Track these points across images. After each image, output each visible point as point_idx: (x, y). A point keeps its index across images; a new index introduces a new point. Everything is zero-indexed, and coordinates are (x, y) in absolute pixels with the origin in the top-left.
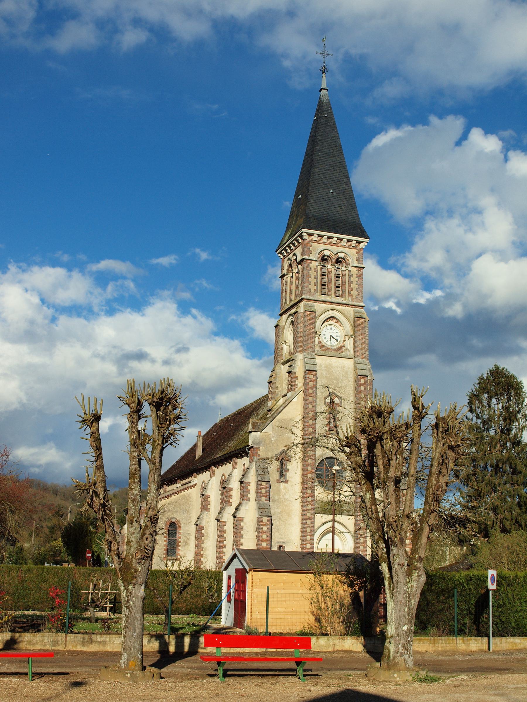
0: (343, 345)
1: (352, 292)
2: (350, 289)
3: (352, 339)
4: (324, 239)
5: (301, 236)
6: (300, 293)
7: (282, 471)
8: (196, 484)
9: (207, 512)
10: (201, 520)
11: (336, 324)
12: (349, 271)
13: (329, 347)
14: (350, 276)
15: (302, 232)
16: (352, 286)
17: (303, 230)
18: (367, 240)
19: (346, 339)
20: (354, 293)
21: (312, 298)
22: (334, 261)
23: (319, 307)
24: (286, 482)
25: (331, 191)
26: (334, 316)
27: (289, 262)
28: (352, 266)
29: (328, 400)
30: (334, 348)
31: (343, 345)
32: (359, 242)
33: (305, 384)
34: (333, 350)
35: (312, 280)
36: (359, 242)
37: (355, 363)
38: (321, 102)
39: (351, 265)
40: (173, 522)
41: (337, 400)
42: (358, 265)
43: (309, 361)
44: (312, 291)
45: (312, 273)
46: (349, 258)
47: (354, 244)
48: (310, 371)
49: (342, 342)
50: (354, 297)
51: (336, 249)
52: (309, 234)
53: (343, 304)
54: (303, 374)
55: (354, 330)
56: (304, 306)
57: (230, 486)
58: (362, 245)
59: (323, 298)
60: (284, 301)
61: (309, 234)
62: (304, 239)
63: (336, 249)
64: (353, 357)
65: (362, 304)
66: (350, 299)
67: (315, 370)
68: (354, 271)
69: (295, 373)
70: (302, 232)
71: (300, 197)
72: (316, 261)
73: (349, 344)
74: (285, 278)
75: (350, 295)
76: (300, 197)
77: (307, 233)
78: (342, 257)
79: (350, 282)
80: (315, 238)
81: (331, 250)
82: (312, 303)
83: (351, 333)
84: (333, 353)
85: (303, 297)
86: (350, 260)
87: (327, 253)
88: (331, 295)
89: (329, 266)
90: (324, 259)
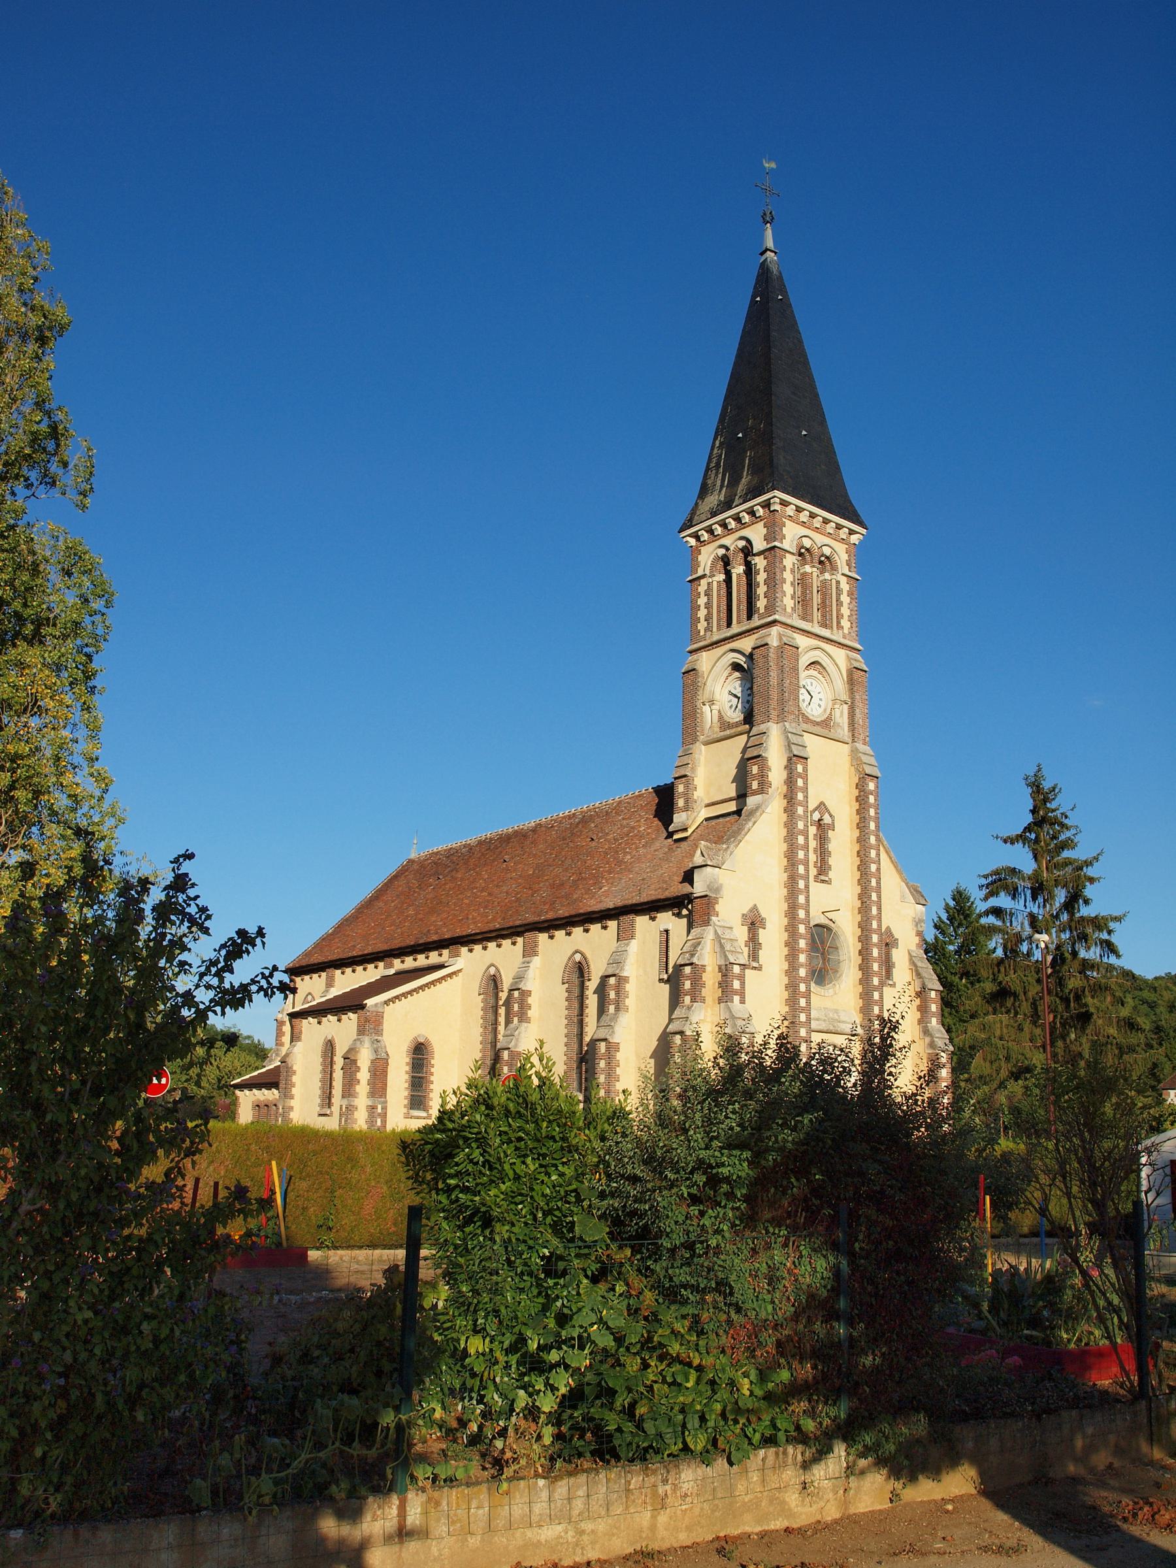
0: (829, 718)
3: (846, 707)
4: (804, 517)
5: (767, 505)
6: (762, 610)
7: (754, 942)
8: (460, 971)
9: (524, 1025)
10: (517, 1040)
11: (820, 676)
12: (838, 582)
13: (811, 717)
14: (839, 591)
15: (775, 497)
17: (777, 493)
18: (864, 531)
19: (836, 706)
20: (845, 623)
21: (789, 621)
22: (816, 560)
23: (802, 641)
24: (759, 968)
25: (804, 433)
26: (820, 661)
27: (722, 552)
28: (843, 574)
29: (816, 816)
30: (818, 720)
31: (829, 718)
32: (852, 532)
33: (790, 782)
34: (818, 724)
35: (788, 589)
36: (852, 532)
37: (854, 753)
38: (764, 269)
40: (422, 1044)
41: (827, 819)
42: (850, 574)
43: (793, 738)
44: (789, 610)
45: (788, 576)
46: (837, 558)
48: (795, 759)
49: (828, 712)
50: (846, 631)
51: (820, 539)
52: (784, 503)
53: (832, 641)
54: (785, 762)
55: (852, 691)
56: (780, 636)
57: (625, 974)
58: (855, 539)
60: (702, 625)
61: (784, 503)
62: (774, 511)
64: (850, 741)
67: (805, 756)
68: (843, 580)
69: (765, 759)
70: (775, 497)
71: (740, 435)
72: (793, 554)
73: (841, 716)
74: (704, 582)
75: (839, 627)
76: (740, 435)
78: (828, 555)
79: (840, 604)
80: (790, 511)
82: (789, 632)
83: (845, 697)
84: (817, 729)
85: (776, 617)
86: (838, 561)
87: (807, 543)
89: (808, 568)
90: (803, 554)
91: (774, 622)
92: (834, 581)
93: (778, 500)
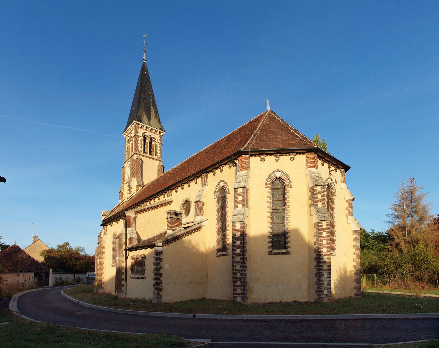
1: (157, 154)
2: (156, 153)
12: (156, 145)
14: (156, 146)
16: (157, 151)
17: (135, 121)
32: (160, 133)
39: (157, 141)
42: (160, 142)
44: (140, 150)
47: (158, 132)
51: (151, 134)
58: (162, 134)
59: (144, 154)
63: (151, 134)
65: (162, 160)
66: (156, 157)
75: (156, 155)
77: (136, 123)
79: (156, 150)
81: (148, 134)
88: (148, 154)
91: (135, 153)
92: (155, 144)
93: (136, 123)
